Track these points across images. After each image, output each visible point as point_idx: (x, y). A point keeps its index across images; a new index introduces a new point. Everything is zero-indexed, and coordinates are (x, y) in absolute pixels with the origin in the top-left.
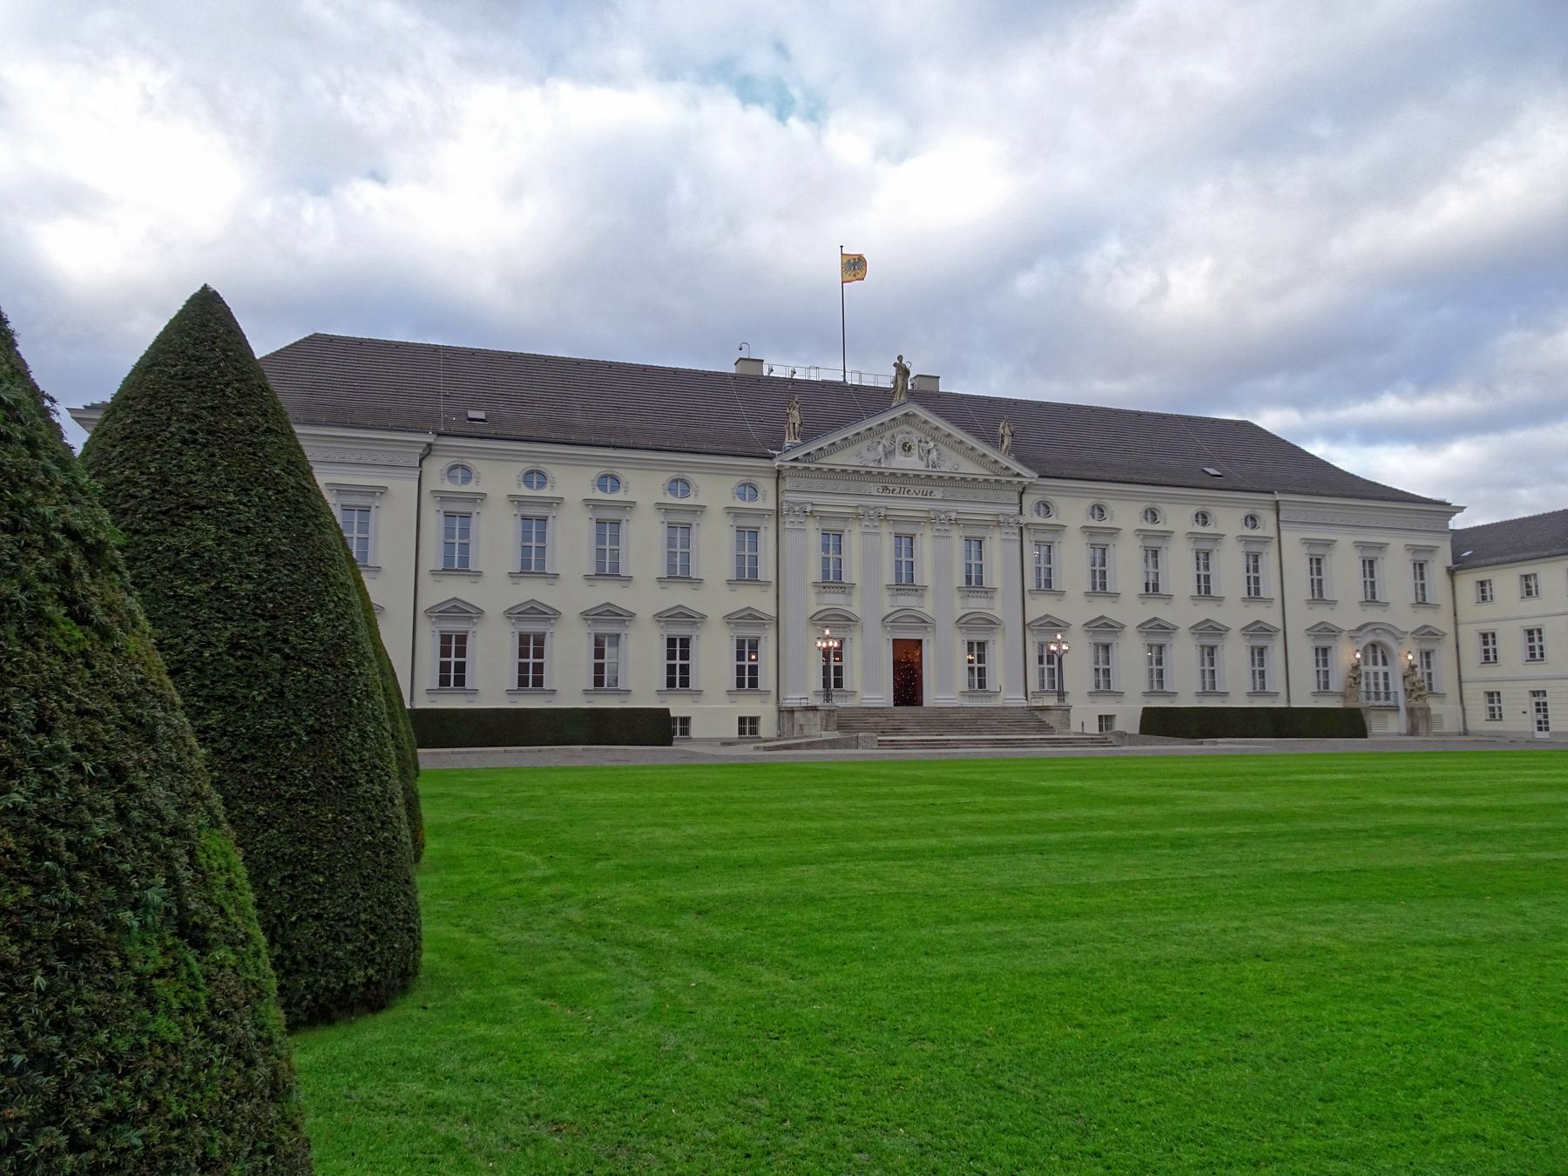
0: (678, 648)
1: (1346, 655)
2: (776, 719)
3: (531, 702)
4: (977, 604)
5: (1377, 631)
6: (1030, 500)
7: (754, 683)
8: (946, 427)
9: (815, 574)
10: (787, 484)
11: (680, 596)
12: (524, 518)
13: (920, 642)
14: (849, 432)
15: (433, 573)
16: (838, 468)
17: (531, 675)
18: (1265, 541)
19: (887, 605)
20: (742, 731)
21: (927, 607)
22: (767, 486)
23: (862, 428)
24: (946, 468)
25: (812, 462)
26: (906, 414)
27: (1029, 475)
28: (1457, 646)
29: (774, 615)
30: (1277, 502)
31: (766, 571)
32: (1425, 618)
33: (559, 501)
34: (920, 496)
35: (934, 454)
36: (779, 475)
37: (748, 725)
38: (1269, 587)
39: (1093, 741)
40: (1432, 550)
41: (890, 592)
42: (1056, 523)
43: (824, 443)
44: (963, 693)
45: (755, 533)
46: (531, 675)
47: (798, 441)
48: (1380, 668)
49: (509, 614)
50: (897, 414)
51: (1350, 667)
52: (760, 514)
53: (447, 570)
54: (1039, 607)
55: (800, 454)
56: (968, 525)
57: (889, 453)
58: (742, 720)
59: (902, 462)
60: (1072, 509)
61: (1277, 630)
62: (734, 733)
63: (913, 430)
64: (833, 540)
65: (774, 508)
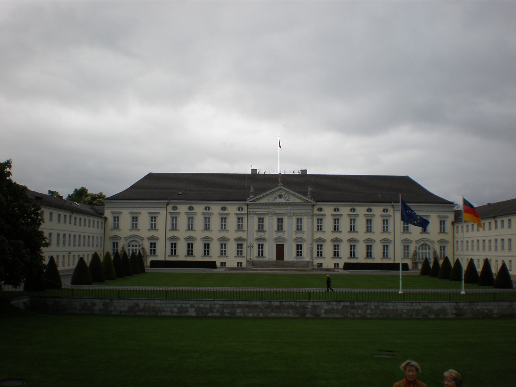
0: (223, 247)
1: (412, 248)
2: (246, 263)
4: (299, 235)
5: (425, 241)
6: (316, 208)
7: (241, 254)
8: (290, 191)
9: (256, 228)
10: (249, 207)
11: (223, 234)
12: (188, 217)
13: (283, 245)
14: (264, 194)
15: (169, 230)
16: (261, 203)
17: (190, 252)
18: (389, 216)
19: (275, 236)
20: (238, 265)
21: (286, 236)
22: (245, 207)
23: (267, 193)
25: (254, 202)
26: (280, 188)
27: (313, 202)
28: (454, 245)
29: (246, 239)
30: (393, 205)
31: (245, 228)
32: (443, 236)
33: (196, 213)
34: (284, 208)
35: (288, 197)
36: (248, 205)
37: (240, 264)
38: (391, 228)
40: (447, 217)
41: (275, 233)
42: (324, 213)
43: (258, 197)
44: (295, 257)
45: (242, 219)
46: (190, 252)
47: (253, 196)
48: (427, 251)
49: (185, 239)
50: (277, 188)
51: (414, 251)
52: (243, 214)
54: (317, 235)
55: (252, 200)
56: (297, 215)
57: (276, 198)
58: (238, 263)
59: (279, 200)
60: (328, 210)
61: (391, 241)
62: (236, 265)
63: (282, 192)
64: (261, 220)
65: (247, 213)
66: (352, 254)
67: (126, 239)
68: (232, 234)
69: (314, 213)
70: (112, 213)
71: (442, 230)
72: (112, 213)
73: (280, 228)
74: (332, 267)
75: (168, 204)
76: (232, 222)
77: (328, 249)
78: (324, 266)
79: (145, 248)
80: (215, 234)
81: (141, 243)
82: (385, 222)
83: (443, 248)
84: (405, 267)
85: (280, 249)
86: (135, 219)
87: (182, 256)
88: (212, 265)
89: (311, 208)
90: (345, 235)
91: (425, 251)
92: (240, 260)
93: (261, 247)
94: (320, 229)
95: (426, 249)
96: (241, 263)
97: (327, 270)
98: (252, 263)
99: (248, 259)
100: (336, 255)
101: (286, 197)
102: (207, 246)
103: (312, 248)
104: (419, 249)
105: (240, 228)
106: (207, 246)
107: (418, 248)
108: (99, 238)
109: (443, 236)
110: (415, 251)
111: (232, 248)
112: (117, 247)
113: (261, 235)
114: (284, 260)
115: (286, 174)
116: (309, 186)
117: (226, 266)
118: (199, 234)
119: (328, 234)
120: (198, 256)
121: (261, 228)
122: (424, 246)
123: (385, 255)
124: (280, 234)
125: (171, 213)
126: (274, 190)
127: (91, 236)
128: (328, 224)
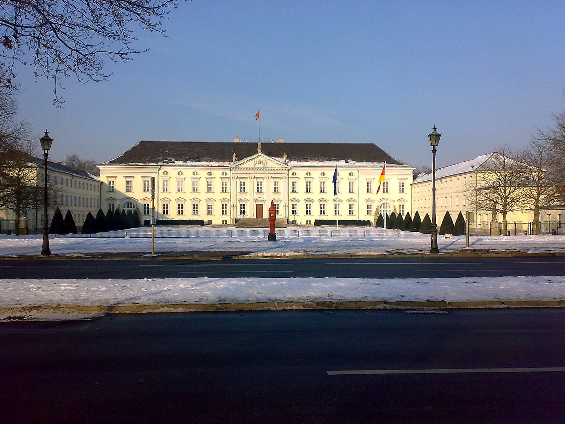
3: (180, 218)
9: (239, 190)
13: (263, 205)
17: (180, 212)
20: (223, 223)
22: (228, 172)
24: (269, 166)
29: (230, 200)
31: (228, 190)
38: (356, 189)
39: (304, 226)
46: (180, 212)
50: (257, 155)
53: (164, 191)
58: (223, 221)
59: (258, 166)
62: (222, 224)
66: (322, 213)
67: (122, 200)
68: (217, 195)
69: (289, 177)
70: (108, 177)
71: (402, 191)
72: (108, 177)
73: (259, 190)
74: (305, 223)
75: (159, 169)
76: (217, 186)
77: (301, 209)
78: (298, 223)
79: (139, 208)
80: (203, 195)
81: (135, 204)
82: (351, 184)
83: (402, 207)
84: (368, 223)
85: (259, 208)
86: (128, 184)
87: (173, 215)
88: (201, 223)
89: (286, 172)
90: (315, 195)
91: (386, 209)
92: (225, 218)
93: (243, 206)
94: (293, 191)
95: (386, 208)
96: (226, 221)
97: (301, 226)
98: (236, 221)
99: (232, 218)
100: (308, 213)
101: (265, 163)
102: (195, 207)
103: (287, 206)
104: (381, 208)
105: (224, 190)
106: (195, 207)
107: (380, 206)
108: (96, 200)
109: (402, 196)
110: (377, 209)
111: (217, 209)
112: (113, 208)
113: (243, 195)
114: (264, 218)
115: (266, 142)
116: (285, 154)
117: (213, 223)
118: (188, 195)
119: (301, 194)
120: (188, 215)
121: (242, 190)
122: (385, 205)
123: (351, 213)
124: (260, 195)
125: (162, 178)
126: (254, 157)
127: (89, 198)
128: (301, 186)
